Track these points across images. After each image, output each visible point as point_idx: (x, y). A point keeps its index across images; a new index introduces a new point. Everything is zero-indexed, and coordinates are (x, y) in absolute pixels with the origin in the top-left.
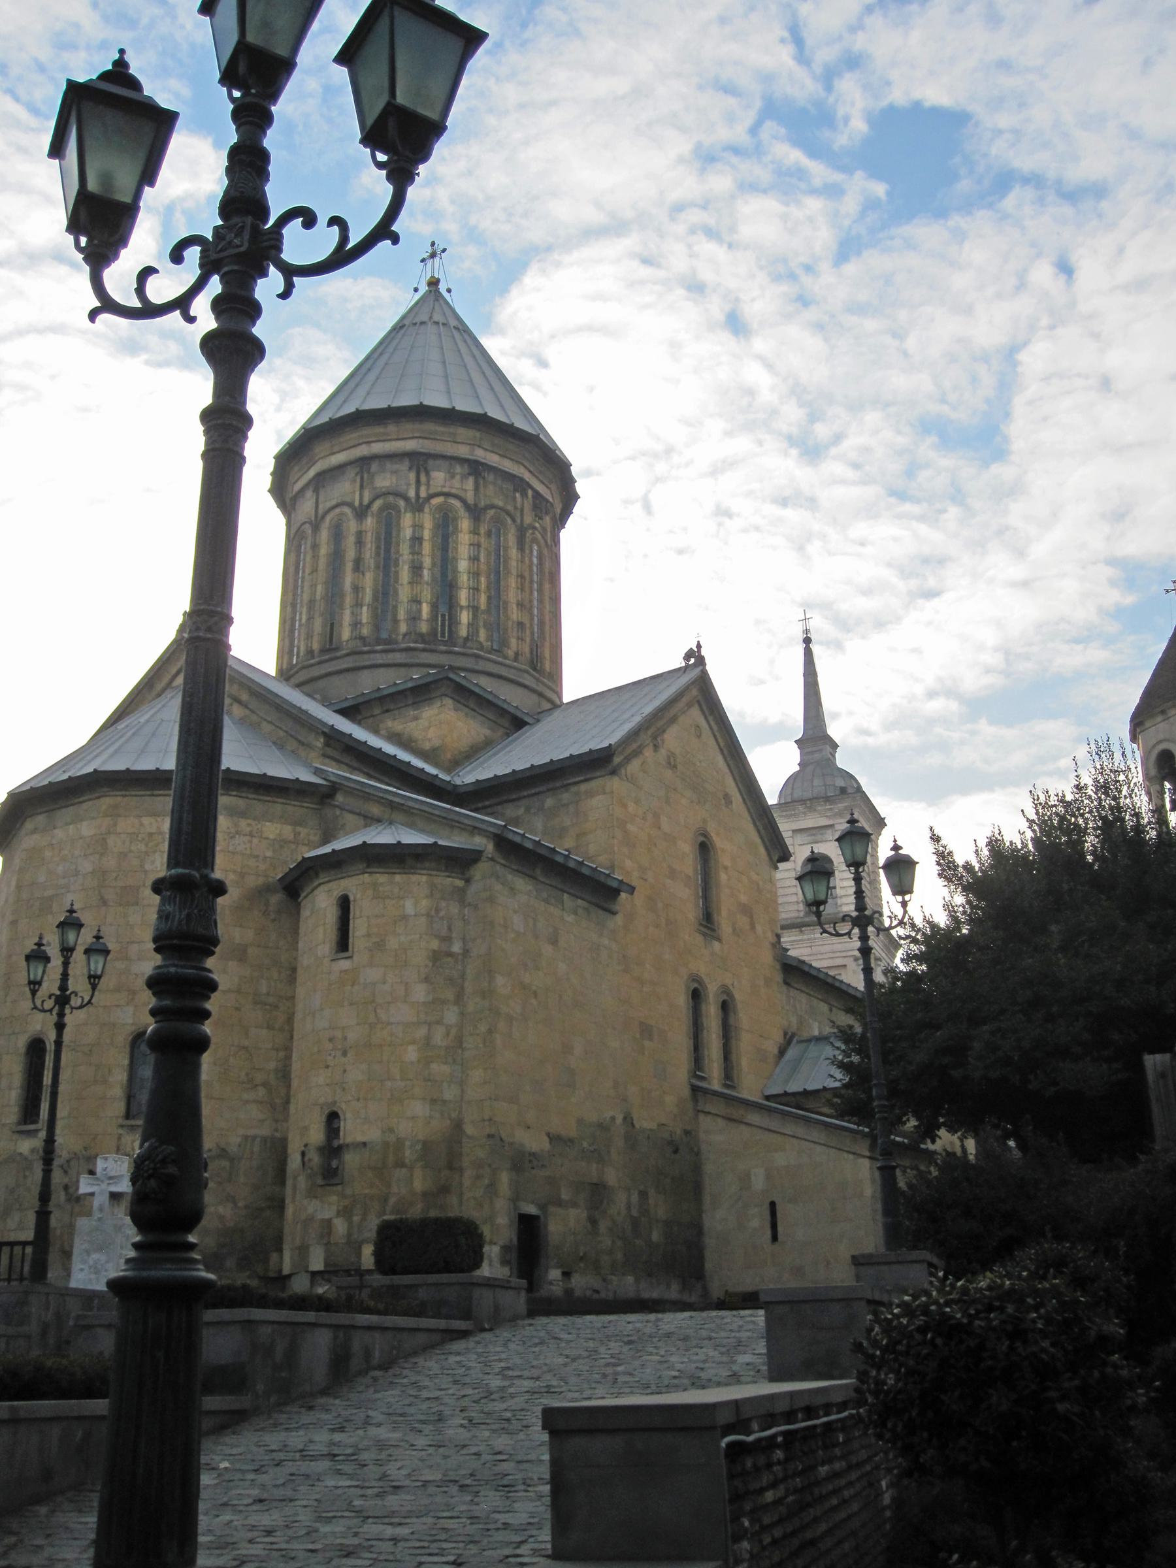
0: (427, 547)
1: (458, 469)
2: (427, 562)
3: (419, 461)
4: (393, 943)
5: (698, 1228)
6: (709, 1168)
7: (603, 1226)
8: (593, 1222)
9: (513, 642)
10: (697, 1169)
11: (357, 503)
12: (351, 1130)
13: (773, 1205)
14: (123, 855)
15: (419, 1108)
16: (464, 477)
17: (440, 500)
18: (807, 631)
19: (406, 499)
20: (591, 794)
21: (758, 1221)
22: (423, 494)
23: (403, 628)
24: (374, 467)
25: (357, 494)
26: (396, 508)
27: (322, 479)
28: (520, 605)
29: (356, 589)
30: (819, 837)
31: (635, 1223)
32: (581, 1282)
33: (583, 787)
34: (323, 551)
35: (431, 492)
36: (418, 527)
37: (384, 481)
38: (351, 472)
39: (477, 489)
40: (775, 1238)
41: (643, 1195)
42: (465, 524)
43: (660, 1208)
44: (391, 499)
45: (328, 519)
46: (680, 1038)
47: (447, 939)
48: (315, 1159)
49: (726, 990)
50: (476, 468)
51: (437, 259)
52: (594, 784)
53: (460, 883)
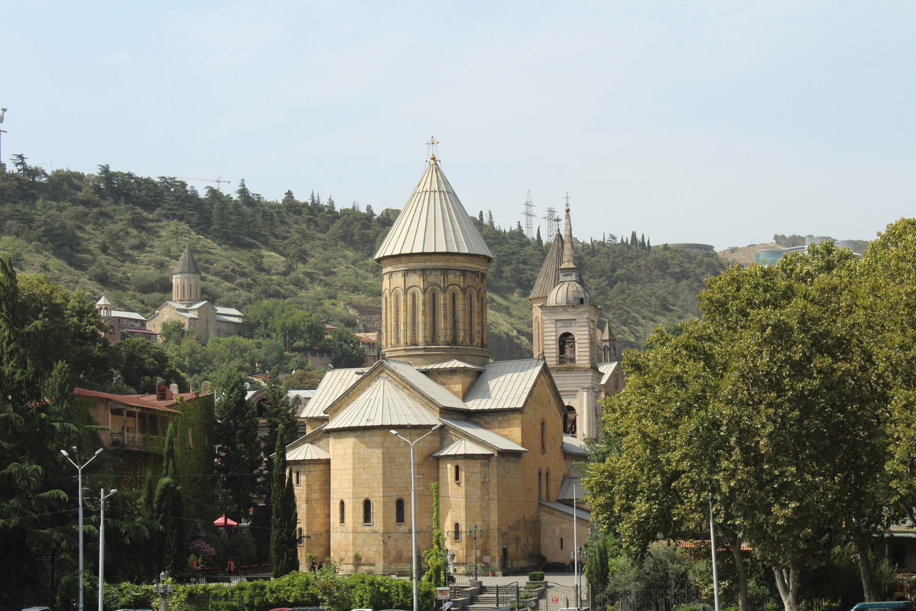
0: (448, 306)
1: (457, 273)
2: (448, 313)
3: (445, 271)
4: (472, 479)
5: (538, 545)
6: (543, 527)
7: (519, 548)
8: (517, 547)
9: (476, 339)
10: (539, 527)
11: (422, 287)
12: (463, 528)
13: (562, 539)
14: (388, 448)
15: (479, 523)
16: (460, 276)
17: (452, 287)
18: (567, 205)
19: (439, 286)
20: (514, 419)
21: (557, 543)
22: (446, 285)
23: (442, 339)
24: (428, 273)
25: (422, 283)
26: (436, 290)
27: (406, 273)
28: (478, 324)
29: (425, 323)
30: (568, 325)
31: (525, 545)
32: (515, 564)
33: (511, 416)
34: (408, 303)
35: (449, 283)
36: (445, 299)
37: (432, 279)
38: (419, 273)
39: (464, 282)
40: (562, 548)
41: (527, 538)
42: (460, 296)
43: (531, 542)
44: (434, 287)
45: (410, 291)
46: (536, 489)
47: (485, 478)
48: (453, 535)
49: (548, 469)
50: (463, 272)
51: (434, 145)
52: (515, 416)
53: (487, 462)
